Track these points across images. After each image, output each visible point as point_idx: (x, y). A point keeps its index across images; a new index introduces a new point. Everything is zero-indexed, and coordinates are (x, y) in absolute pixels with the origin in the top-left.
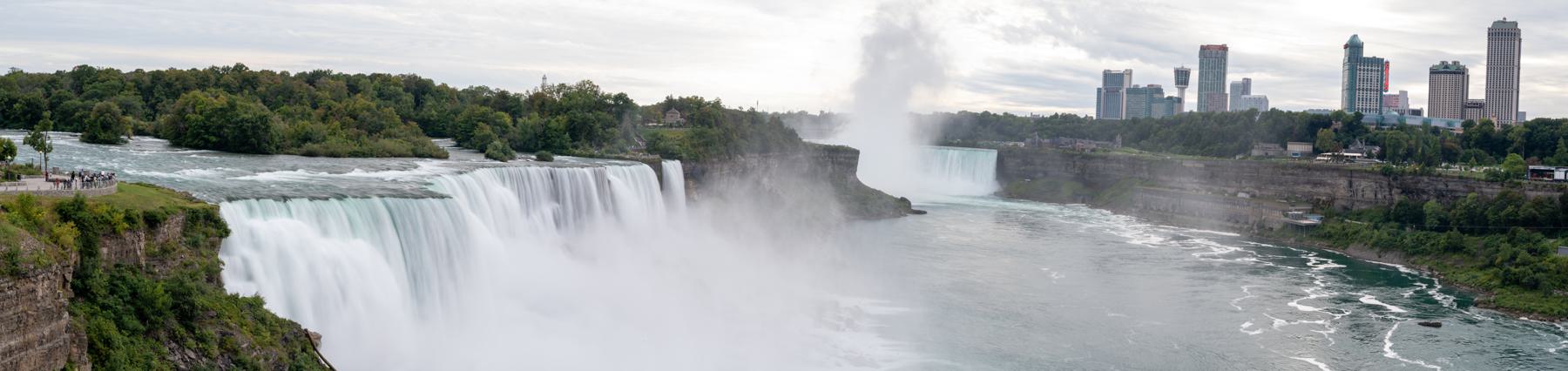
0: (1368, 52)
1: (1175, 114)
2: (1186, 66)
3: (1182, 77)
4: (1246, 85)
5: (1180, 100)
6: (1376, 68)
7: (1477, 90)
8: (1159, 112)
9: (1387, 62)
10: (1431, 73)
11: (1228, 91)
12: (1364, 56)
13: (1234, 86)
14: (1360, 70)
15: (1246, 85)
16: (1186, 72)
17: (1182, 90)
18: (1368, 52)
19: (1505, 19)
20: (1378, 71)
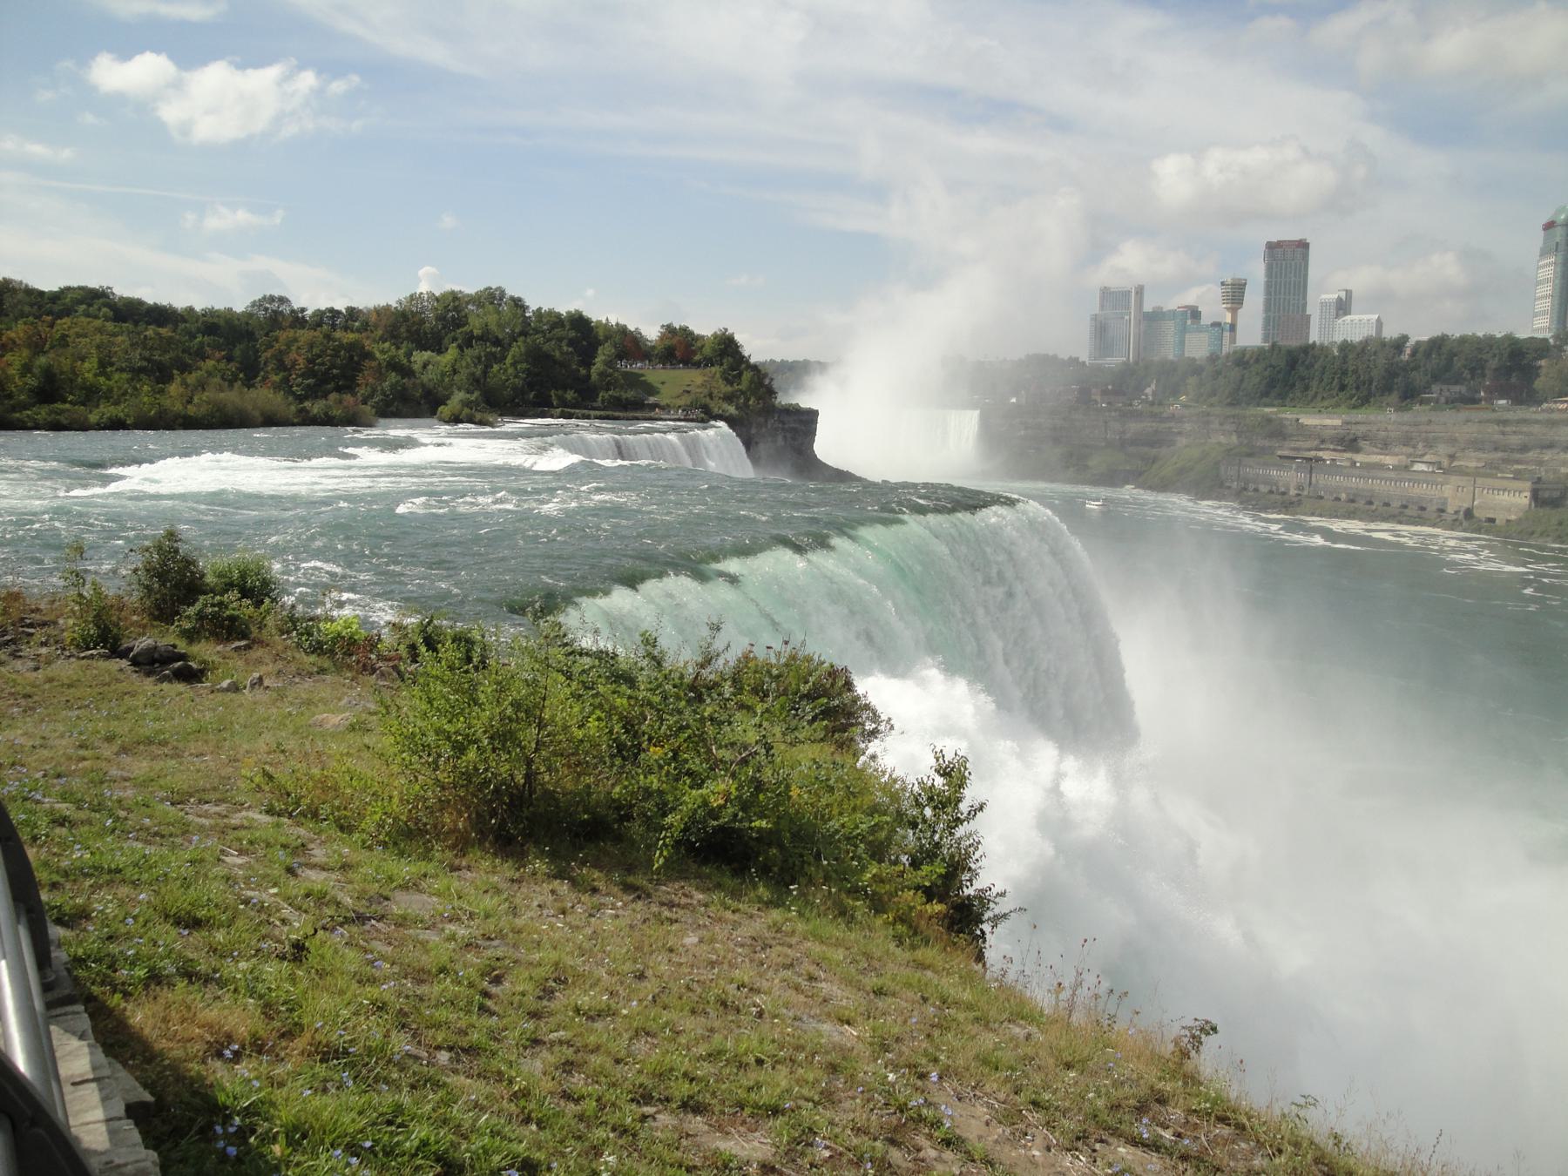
1: (1226, 349)
3: (1235, 294)
4: (1343, 306)
5: (1233, 327)
8: (1198, 348)
11: (1313, 309)
13: (1323, 304)
17: (1234, 311)
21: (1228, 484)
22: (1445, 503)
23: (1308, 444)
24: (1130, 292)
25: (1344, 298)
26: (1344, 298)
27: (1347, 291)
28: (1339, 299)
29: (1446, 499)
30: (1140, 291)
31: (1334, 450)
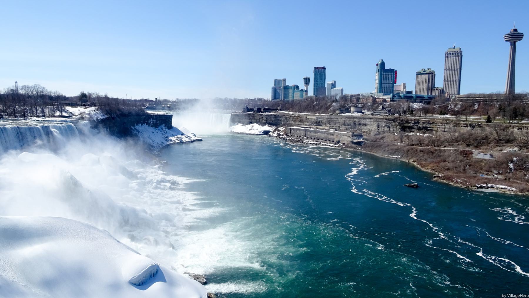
0: (387, 67)
2: (308, 77)
3: (307, 81)
4: (333, 85)
5: (306, 91)
6: (391, 74)
7: (439, 83)
9: (396, 71)
10: (417, 74)
11: (326, 86)
12: (385, 69)
13: (328, 85)
14: (384, 75)
15: (333, 85)
16: (308, 79)
18: (387, 67)
19: (454, 47)
20: (392, 75)
21: (288, 135)
22: (334, 140)
23: (308, 124)
24: (282, 81)
25: (333, 83)
26: (333, 83)
27: (334, 81)
28: (332, 83)
29: (334, 138)
30: (285, 80)
31: (315, 125)
